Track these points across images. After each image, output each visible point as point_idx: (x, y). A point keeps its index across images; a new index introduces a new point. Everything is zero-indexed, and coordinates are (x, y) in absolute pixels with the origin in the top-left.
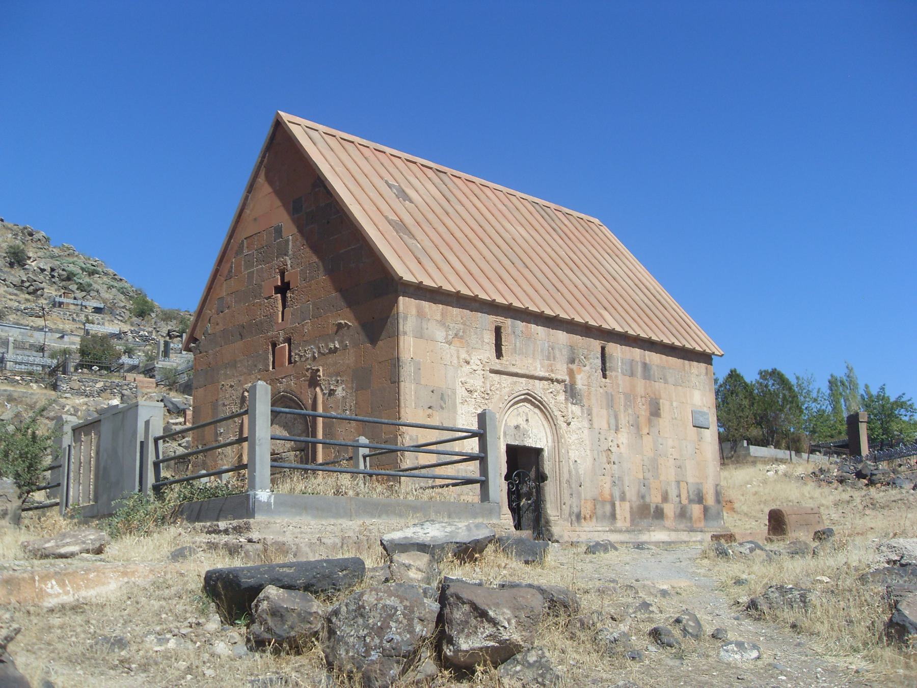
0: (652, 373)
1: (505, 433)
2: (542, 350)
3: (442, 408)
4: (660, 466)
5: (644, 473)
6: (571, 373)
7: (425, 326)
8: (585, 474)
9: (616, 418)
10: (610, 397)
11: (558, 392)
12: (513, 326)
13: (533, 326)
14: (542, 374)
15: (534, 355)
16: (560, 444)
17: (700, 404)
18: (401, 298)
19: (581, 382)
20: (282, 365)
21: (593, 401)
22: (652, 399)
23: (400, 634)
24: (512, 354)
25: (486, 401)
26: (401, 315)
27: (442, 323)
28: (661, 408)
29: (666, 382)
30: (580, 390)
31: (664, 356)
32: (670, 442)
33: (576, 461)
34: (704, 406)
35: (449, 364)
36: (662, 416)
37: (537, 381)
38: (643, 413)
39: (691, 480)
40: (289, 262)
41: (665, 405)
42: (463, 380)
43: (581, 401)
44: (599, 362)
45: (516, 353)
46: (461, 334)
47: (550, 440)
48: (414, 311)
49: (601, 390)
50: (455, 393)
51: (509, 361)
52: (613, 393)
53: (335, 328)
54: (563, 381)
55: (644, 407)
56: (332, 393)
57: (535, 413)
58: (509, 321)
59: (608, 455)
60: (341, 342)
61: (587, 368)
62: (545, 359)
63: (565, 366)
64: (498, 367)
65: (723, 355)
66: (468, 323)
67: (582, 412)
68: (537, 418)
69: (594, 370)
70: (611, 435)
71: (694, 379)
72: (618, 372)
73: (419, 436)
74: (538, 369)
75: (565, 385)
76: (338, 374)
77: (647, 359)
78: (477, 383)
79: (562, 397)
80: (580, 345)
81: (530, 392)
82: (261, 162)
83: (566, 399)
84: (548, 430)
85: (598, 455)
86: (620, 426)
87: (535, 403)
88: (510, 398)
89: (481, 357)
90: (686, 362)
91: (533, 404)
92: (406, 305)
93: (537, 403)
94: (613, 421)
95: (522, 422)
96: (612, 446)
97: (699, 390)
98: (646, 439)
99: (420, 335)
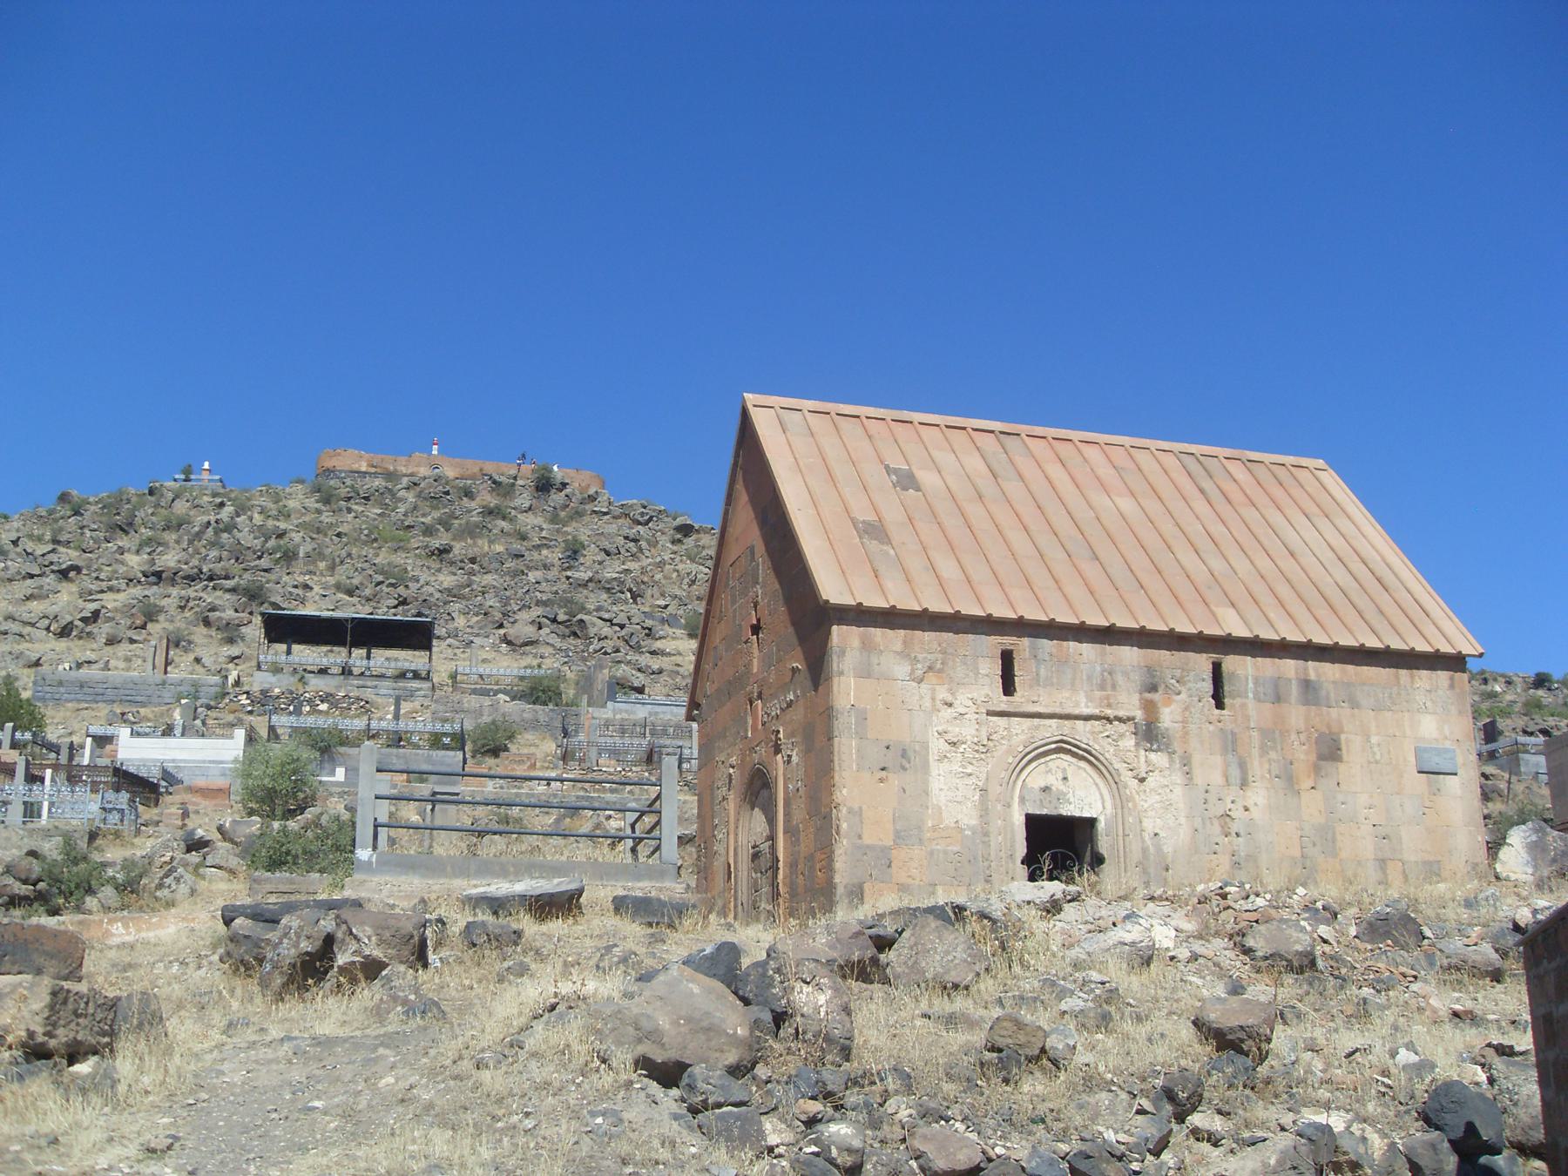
0: (1323, 693)
1: (1022, 800)
2: (1089, 678)
3: (904, 769)
4: (1339, 837)
5: (1302, 848)
6: (1150, 708)
7: (874, 660)
8: (1175, 852)
9: (1243, 766)
10: (1230, 737)
11: (1122, 736)
13: (1071, 643)
15: (1073, 684)
16: (1126, 810)
17: (1435, 734)
18: (835, 628)
19: (1168, 717)
20: (757, 729)
22: (1321, 735)
23: (288, 949)
24: (1031, 687)
25: (983, 756)
26: (836, 649)
27: (906, 654)
29: (1354, 704)
30: (1167, 729)
31: (1350, 668)
32: (1363, 799)
33: (1156, 834)
35: (918, 708)
37: (1079, 723)
38: (1302, 757)
39: (1410, 857)
40: (760, 592)
42: (940, 729)
43: (1168, 745)
44: (1208, 687)
45: (1039, 685)
46: (939, 666)
47: (1109, 804)
48: (856, 643)
49: (1211, 728)
50: (927, 748)
52: (1236, 731)
53: (791, 673)
54: (1130, 719)
55: (1304, 747)
56: (789, 756)
57: (1080, 768)
58: (1026, 641)
59: (1226, 823)
60: (795, 693)
61: (1183, 696)
62: (1094, 688)
63: (1137, 696)
64: (1003, 707)
65: (1481, 655)
66: (950, 650)
67: (1171, 761)
68: (1085, 775)
69: (1196, 699)
70: (1234, 791)
71: (1420, 698)
72: (1247, 697)
73: (864, 807)
75: (1135, 723)
76: (792, 735)
78: (967, 731)
79: (1129, 742)
81: (1065, 738)
82: (735, 464)
83: (1137, 744)
84: (1105, 791)
85: (1204, 823)
86: (1251, 779)
87: (1077, 754)
88: (1028, 750)
89: (975, 695)
90: (1403, 672)
91: (1074, 755)
92: (841, 635)
93: (1081, 752)
94: (1235, 773)
95: (1055, 782)
96: (1234, 809)
97: (1435, 713)
98: (1305, 796)
99: (865, 673)
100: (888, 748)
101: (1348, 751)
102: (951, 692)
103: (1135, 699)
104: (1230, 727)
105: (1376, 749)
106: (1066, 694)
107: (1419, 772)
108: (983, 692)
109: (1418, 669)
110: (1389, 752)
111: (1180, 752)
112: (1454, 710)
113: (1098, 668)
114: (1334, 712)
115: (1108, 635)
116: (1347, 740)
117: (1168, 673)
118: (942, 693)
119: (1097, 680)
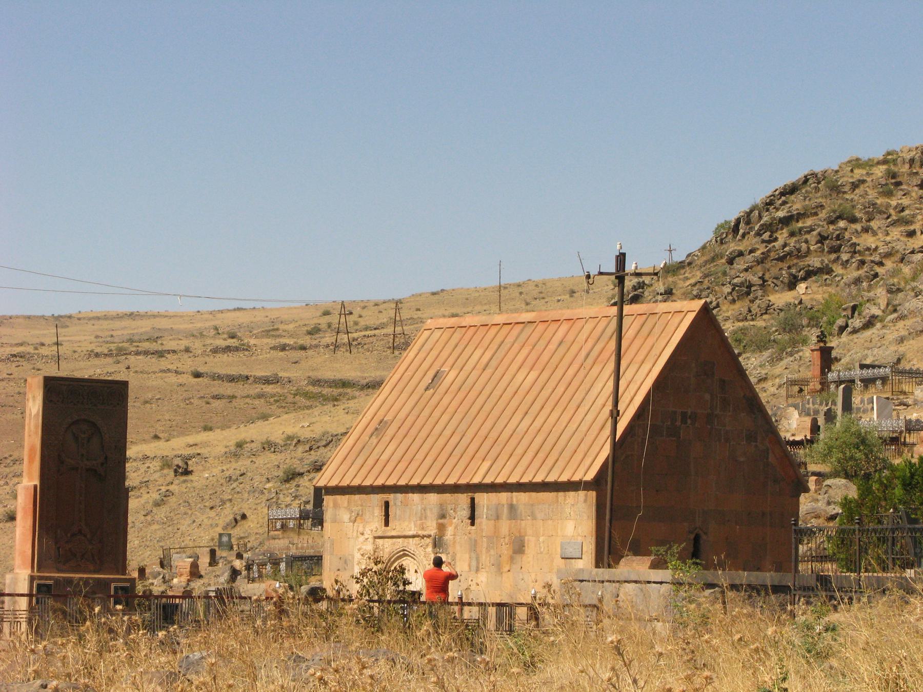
0: (519, 511)
2: (416, 514)
6: (441, 528)
11: (427, 545)
12: (395, 499)
13: (410, 494)
14: (411, 533)
15: (409, 518)
21: (458, 547)
28: (526, 545)
30: (447, 540)
31: (534, 494)
34: (579, 535)
36: (526, 552)
37: (411, 540)
41: (530, 541)
42: (358, 547)
44: (466, 513)
45: (396, 519)
48: (331, 505)
51: (396, 527)
55: (508, 546)
57: (415, 564)
66: (364, 505)
69: (460, 521)
71: (568, 510)
74: (413, 529)
77: (514, 499)
80: (448, 502)
81: (405, 548)
86: (481, 567)
90: (561, 494)
94: (474, 563)
99: (334, 521)
100: (340, 558)
101: (528, 546)
102: (364, 528)
103: (434, 524)
104: (473, 536)
105: (542, 545)
106: (406, 523)
107: (562, 558)
108: (375, 526)
109: (568, 491)
110: (548, 547)
111: (451, 553)
112: (585, 518)
113: (420, 508)
114: (523, 523)
115: (421, 489)
116: (528, 541)
117: (449, 507)
118: (361, 529)
119: (419, 515)
